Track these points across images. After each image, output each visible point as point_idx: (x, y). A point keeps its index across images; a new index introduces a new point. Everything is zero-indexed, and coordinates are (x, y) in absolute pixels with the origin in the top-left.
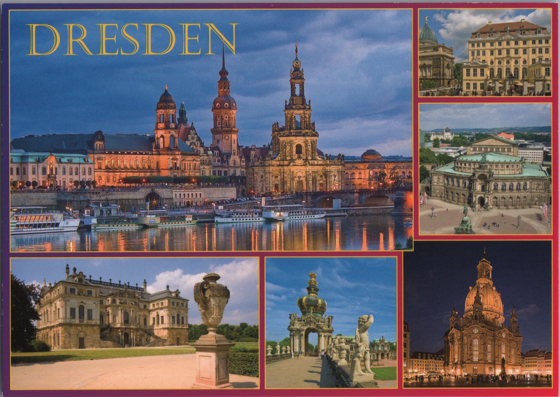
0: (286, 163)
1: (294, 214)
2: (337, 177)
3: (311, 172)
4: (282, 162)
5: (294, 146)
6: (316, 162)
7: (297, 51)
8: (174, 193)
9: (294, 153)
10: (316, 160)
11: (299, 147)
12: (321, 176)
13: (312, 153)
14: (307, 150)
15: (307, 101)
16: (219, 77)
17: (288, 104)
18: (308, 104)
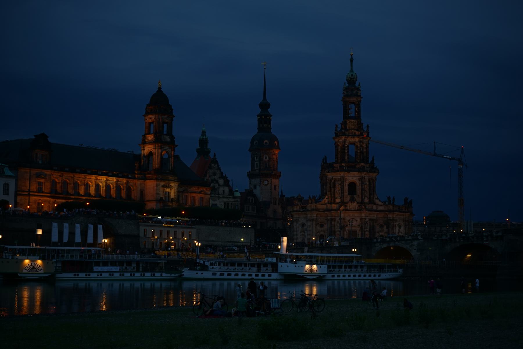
0: (335, 206)
1: (337, 269)
2: (402, 228)
3: (367, 220)
4: (329, 206)
5: (346, 184)
6: (375, 207)
7: (352, 61)
8: (142, 228)
9: (346, 194)
10: (375, 204)
11: (352, 185)
12: (381, 226)
13: (370, 194)
14: (363, 190)
15: (365, 126)
16: (259, 111)
17: (339, 129)
18: (365, 130)
